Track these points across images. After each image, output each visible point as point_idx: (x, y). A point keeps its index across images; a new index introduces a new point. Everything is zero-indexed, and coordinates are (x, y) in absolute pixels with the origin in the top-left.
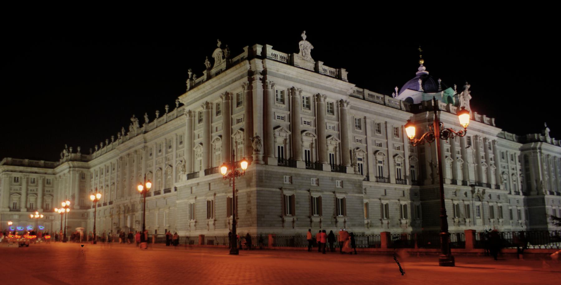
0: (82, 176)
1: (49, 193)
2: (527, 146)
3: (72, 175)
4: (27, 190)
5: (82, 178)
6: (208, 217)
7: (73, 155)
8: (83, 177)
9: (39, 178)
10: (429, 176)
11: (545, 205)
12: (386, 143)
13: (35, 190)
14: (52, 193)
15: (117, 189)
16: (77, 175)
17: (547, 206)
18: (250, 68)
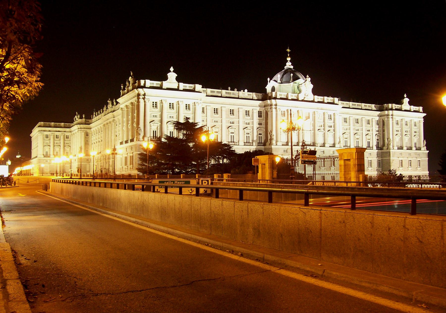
0: (87, 134)
1: (68, 145)
2: (383, 113)
3: (79, 134)
4: (54, 143)
5: (87, 135)
6: (125, 165)
7: (80, 120)
8: (87, 135)
9: (61, 135)
10: (269, 141)
11: (390, 157)
12: (238, 121)
13: (59, 143)
14: (70, 145)
15: (101, 145)
16: (83, 134)
17: (391, 158)
18: (138, 92)
